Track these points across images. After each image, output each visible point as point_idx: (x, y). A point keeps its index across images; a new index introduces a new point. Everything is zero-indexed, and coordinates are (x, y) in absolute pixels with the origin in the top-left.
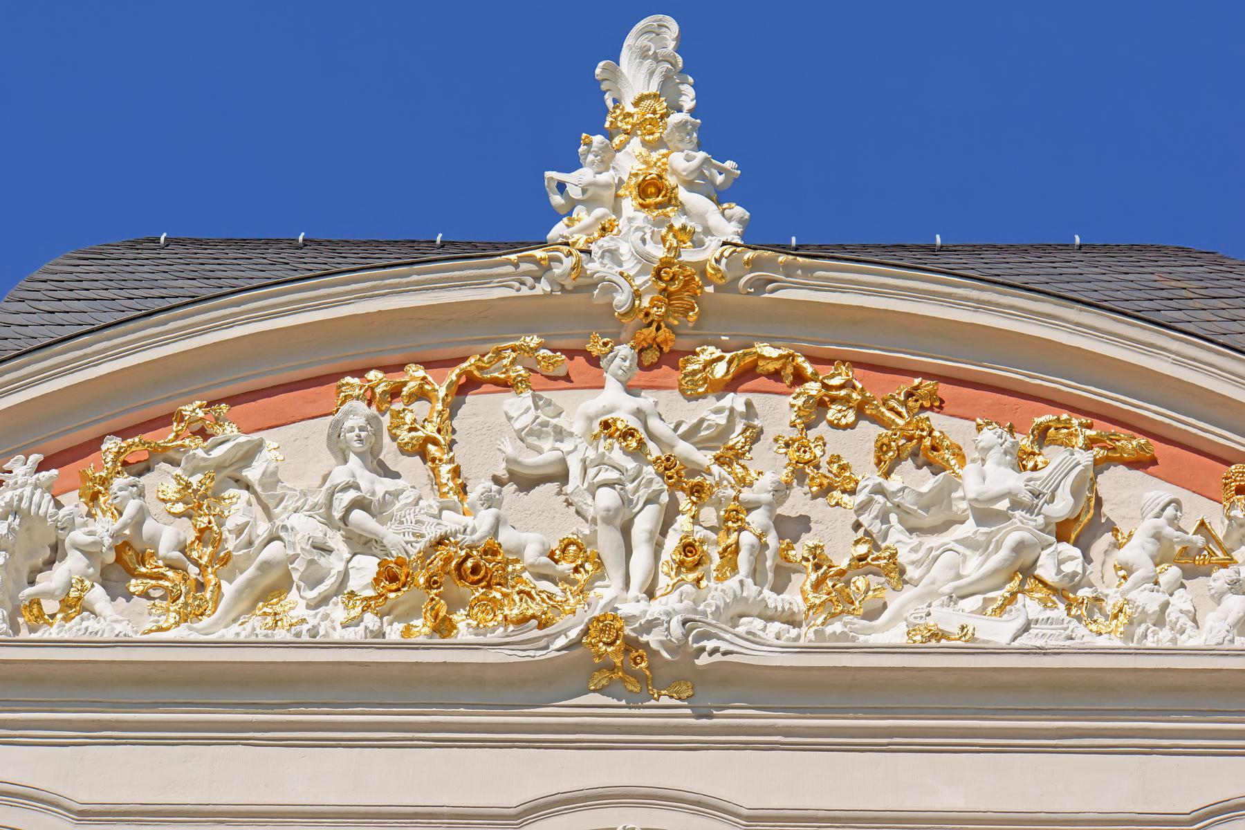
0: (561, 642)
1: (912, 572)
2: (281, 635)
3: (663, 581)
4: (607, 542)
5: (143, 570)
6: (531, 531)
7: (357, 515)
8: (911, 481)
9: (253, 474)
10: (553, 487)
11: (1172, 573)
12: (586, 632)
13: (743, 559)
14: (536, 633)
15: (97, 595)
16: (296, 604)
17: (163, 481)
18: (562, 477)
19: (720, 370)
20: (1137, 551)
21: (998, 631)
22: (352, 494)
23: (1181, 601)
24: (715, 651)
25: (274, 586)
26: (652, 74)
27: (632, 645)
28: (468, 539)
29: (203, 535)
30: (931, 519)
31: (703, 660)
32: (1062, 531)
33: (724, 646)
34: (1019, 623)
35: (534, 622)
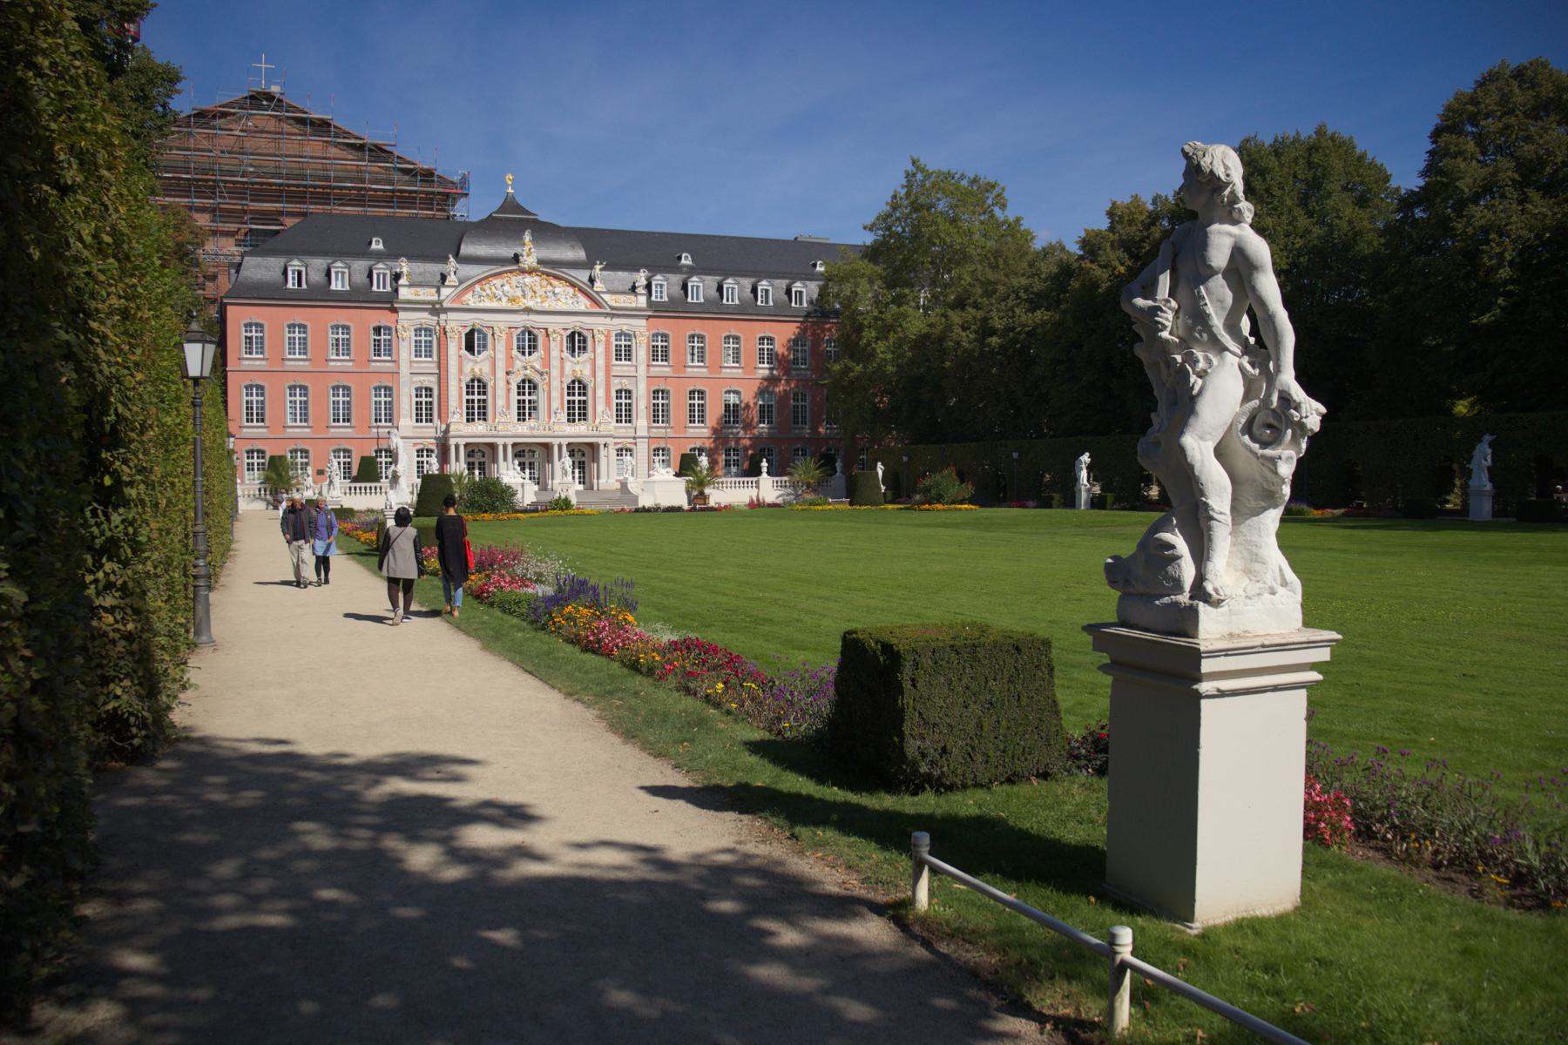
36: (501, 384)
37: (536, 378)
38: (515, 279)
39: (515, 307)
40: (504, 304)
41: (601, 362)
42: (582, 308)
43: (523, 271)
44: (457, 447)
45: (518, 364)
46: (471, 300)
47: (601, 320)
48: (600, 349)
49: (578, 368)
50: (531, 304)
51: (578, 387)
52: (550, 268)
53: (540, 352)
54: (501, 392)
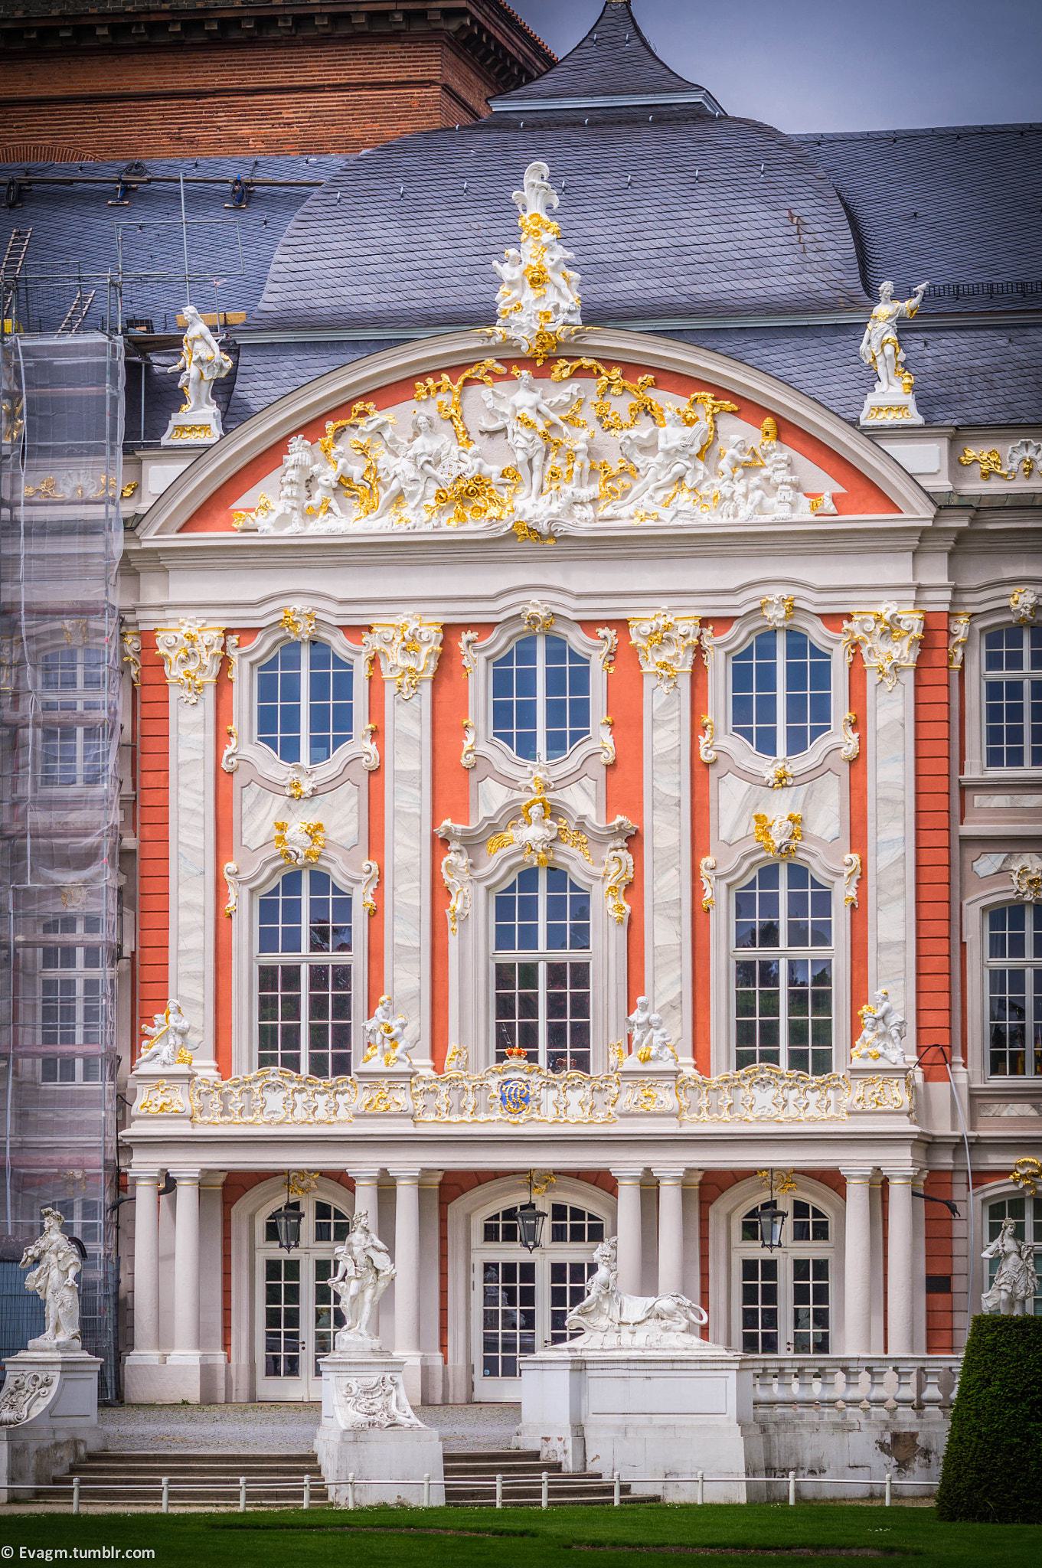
1: (642, 473)
2: (404, 529)
3: (546, 486)
4: (524, 471)
7: (427, 467)
8: (643, 430)
10: (503, 435)
11: (740, 471)
15: (333, 503)
16: (407, 511)
17: (353, 437)
18: (504, 430)
19: (566, 373)
21: (667, 515)
22: (424, 458)
23: (740, 488)
25: (399, 497)
30: (648, 448)
34: (673, 513)
36: (408, 897)
37: (579, 863)
39: (474, 526)
40: (418, 519)
41: (892, 773)
42: (785, 510)
43: (515, 362)
44: (168, 1185)
45: (491, 798)
47: (897, 570)
48: (892, 708)
49: (779, 809)
50: (532, 506)
51: (779, 898)
52: (636, 335)
53: (601, 739)
54: (407, 931)
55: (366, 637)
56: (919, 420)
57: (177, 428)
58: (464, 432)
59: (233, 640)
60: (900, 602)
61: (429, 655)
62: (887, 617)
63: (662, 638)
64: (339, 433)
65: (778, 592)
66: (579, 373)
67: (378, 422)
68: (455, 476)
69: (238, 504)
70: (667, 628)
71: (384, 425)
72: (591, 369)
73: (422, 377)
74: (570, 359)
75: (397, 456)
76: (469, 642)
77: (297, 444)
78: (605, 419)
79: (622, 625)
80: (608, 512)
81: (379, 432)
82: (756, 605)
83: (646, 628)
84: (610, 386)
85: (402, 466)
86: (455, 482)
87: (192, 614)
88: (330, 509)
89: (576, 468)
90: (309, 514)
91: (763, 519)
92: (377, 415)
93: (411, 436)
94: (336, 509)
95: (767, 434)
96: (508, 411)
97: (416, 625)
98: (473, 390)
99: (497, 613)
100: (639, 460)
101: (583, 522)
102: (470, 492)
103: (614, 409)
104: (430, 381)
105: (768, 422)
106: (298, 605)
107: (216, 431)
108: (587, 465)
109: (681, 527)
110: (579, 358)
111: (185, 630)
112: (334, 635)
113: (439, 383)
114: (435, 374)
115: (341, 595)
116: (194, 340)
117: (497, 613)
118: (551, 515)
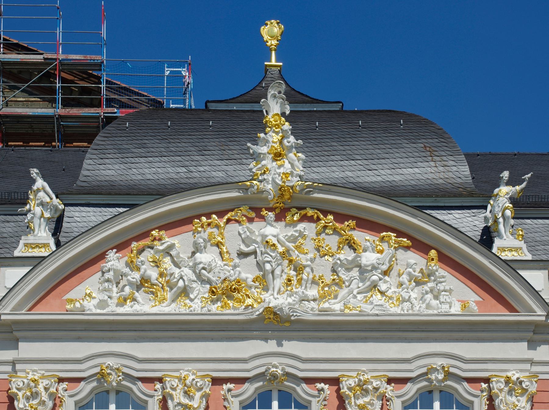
0: (257, 313)
2: (188, 311)
3: (282, 289)
5: (146, 285)
6: (247, 272)
7: (203, 271)
9: (173, 253)
10: (253, 256)
12: (263, 311)
13: (303, 282)
14: (251, 310)
17: (148, 255)
20: (405, 278)
21: (367, 308)
22: (201, 266)
24: (296, 315)
26: (277, 102)
27: (275, 314)
28: (232, 278)
29: (161, 275)
31: (292, 318)
32: (385, 273)
33: (298, 314)
35: (250, 307)
38: (233, 235)
46: (90, 297)
50: (278, 299)
55: (158, 386)
56: (529, 257)
57: (26, 245)
58: (227, 252)
59: (65, 385)
60: (521, 371)
61: (202, 397)
62: (514, 378)
63: (362, 388)
64: (141, 251)
65: (439, 362)
66: (304, 218)
67: (169, 243)
68: (223, 278)
69: (68, 296)
70: (366, 382)
71: (172, 246)
72: (312, 216)
73: (199, 217)
74: (300, 209)
75: (180, 268)
76: (229, 390)
77: (112, 255)
78: (321, 249)
79: (335, 382)
80: (326, 305)
81: (167, 252)
82: (424, 370)
83: (352, 382)
84: (325, 227)
85: (188, 273)
86: (222, 283)
87: (35, 367)
88: (134, 300)
89: (305, 277)
90: (123, 301)
91: (430, 312)
92: (167, 239)
93: (190, 255)
94: (139, 299)
95: (433, 260)
96: (259, 239)
97: (194, 377)
98: (234, 227)
99: (248, 371)
100: (343, 274)
101: (309, 312)
102: (230, 291)
103: (327, 242)
104: (204, 219)
105: (433, 253)
106: (111, 362)
107: (54, 248)
108: (311, 276)
109: (377, 315)
110: (305, 208)
111: (30, 376)
112: (135, 384)
113: (210, 221)
114: (208, 216)
115: (140, 355)
116: (38, 190)
117: (248, 371)
118: (289, 304)
